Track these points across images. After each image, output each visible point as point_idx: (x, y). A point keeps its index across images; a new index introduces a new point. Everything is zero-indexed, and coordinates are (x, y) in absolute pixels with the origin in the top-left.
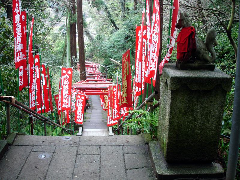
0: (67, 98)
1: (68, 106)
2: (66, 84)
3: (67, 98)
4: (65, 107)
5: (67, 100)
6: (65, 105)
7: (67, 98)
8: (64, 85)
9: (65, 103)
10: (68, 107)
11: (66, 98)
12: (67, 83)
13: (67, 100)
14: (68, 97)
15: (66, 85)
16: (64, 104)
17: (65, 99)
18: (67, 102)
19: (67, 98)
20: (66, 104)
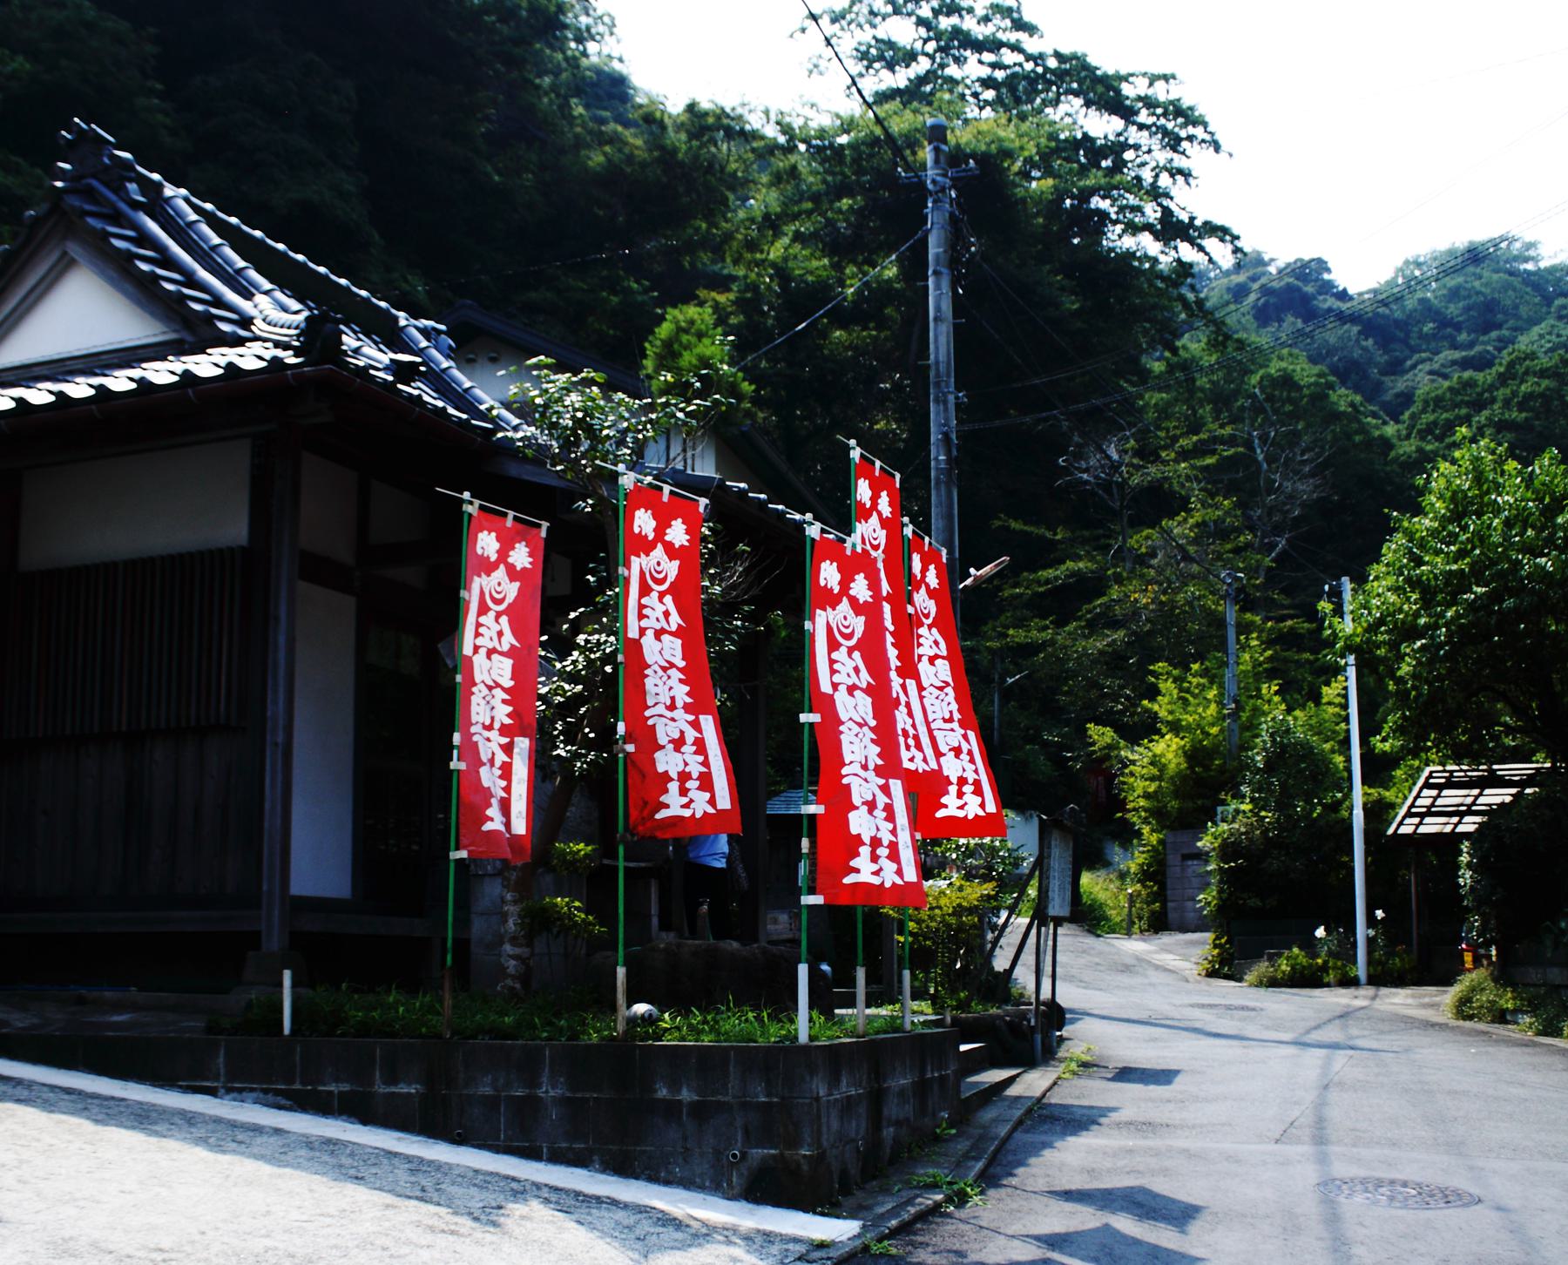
0: (690, 738)
1: (712, 802)
2: (658, 627)
3: (691, 735)
5: (688, 749)
6: (684, 792)
7: (690, 738)
8: (642, 631)
9: (684, 777)
10: (711, 810)
11: (676, 735)
12: (667, 614)
13: (688, 749)
14: (696, 725)
15: (659, 634)
17: (677, 749)
18: (695, 769)
19: (691, 735)
20: (692, 784)
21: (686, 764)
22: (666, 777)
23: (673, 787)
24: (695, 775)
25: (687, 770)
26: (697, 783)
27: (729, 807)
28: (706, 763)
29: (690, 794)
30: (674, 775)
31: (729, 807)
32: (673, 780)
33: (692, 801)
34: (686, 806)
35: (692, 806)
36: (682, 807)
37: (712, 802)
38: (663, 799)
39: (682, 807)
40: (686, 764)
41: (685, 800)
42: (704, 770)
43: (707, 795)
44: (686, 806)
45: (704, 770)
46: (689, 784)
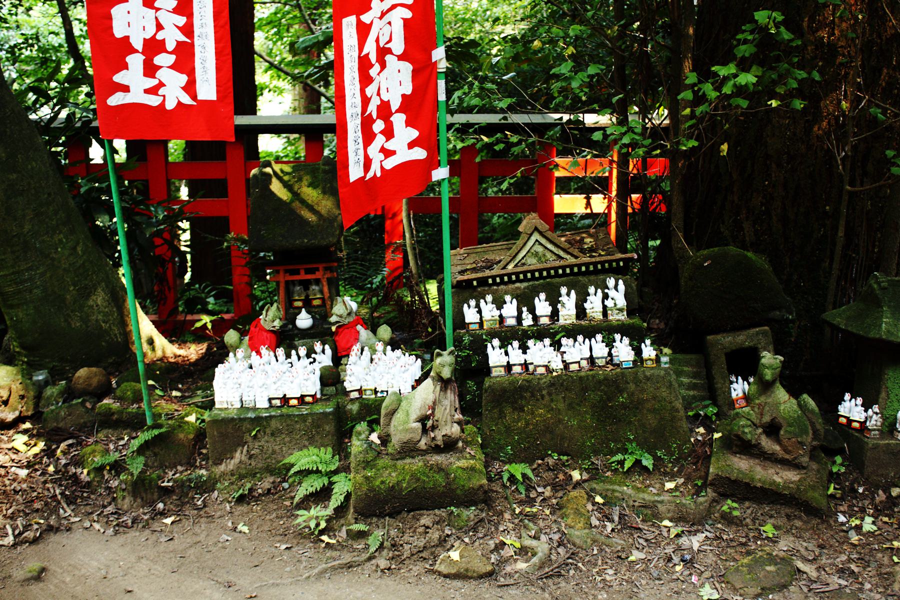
1: (190, 88)
4: (153, 101)
6: (150, 70)
9: (153, 47)
10: (187, 100)
16: (136, 61)
18: (172, 37)
21: (159, 27)
22: (125, 45)
23: (136, 61)
24: (171, 46)
25: (159, 37)
26: (172, 59)
27: (215, 98)
28: (188, 30)
29: (159, 74)
30: (138, 44)
31: (215, 98)
32: (137, 51)
33: (161, 85)
34: (150, 91)
35: (161, 92)
36: (147, 91)
37: (190, 88)
38: (119, 78)
39: (147, 91)
40: (159, 27)
41: (151, 83)
42: (183, 38)
43: (183, 79)
44: (150, 91)
45: (183, 38)
46: (159, 60)
